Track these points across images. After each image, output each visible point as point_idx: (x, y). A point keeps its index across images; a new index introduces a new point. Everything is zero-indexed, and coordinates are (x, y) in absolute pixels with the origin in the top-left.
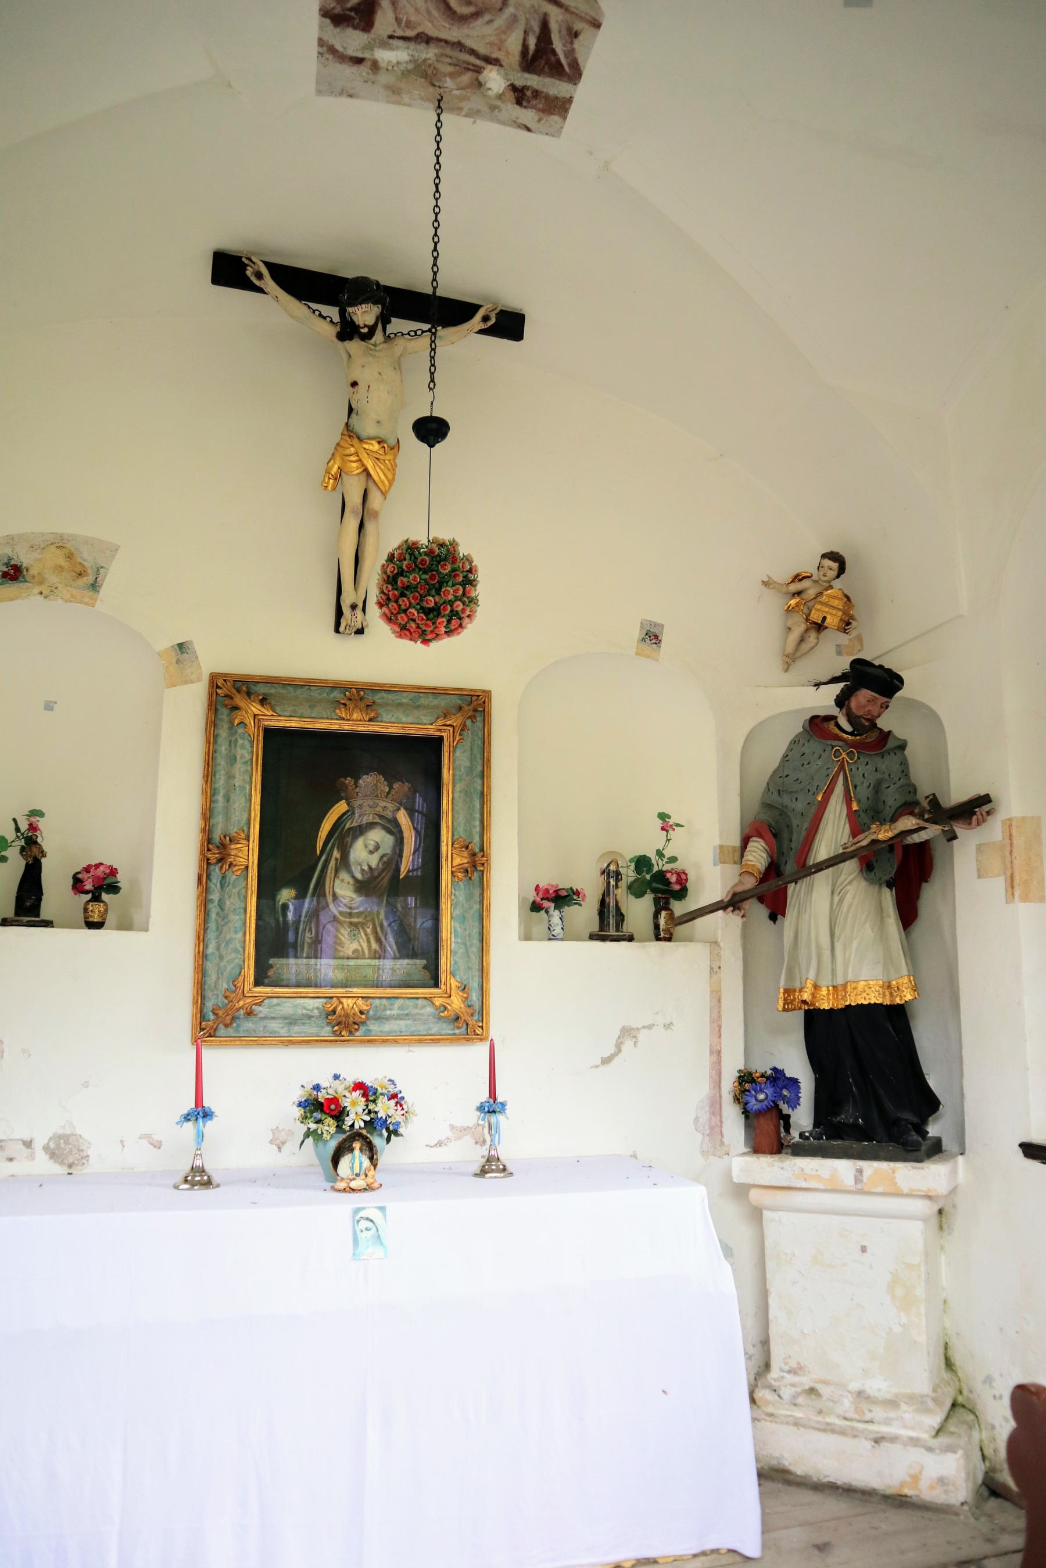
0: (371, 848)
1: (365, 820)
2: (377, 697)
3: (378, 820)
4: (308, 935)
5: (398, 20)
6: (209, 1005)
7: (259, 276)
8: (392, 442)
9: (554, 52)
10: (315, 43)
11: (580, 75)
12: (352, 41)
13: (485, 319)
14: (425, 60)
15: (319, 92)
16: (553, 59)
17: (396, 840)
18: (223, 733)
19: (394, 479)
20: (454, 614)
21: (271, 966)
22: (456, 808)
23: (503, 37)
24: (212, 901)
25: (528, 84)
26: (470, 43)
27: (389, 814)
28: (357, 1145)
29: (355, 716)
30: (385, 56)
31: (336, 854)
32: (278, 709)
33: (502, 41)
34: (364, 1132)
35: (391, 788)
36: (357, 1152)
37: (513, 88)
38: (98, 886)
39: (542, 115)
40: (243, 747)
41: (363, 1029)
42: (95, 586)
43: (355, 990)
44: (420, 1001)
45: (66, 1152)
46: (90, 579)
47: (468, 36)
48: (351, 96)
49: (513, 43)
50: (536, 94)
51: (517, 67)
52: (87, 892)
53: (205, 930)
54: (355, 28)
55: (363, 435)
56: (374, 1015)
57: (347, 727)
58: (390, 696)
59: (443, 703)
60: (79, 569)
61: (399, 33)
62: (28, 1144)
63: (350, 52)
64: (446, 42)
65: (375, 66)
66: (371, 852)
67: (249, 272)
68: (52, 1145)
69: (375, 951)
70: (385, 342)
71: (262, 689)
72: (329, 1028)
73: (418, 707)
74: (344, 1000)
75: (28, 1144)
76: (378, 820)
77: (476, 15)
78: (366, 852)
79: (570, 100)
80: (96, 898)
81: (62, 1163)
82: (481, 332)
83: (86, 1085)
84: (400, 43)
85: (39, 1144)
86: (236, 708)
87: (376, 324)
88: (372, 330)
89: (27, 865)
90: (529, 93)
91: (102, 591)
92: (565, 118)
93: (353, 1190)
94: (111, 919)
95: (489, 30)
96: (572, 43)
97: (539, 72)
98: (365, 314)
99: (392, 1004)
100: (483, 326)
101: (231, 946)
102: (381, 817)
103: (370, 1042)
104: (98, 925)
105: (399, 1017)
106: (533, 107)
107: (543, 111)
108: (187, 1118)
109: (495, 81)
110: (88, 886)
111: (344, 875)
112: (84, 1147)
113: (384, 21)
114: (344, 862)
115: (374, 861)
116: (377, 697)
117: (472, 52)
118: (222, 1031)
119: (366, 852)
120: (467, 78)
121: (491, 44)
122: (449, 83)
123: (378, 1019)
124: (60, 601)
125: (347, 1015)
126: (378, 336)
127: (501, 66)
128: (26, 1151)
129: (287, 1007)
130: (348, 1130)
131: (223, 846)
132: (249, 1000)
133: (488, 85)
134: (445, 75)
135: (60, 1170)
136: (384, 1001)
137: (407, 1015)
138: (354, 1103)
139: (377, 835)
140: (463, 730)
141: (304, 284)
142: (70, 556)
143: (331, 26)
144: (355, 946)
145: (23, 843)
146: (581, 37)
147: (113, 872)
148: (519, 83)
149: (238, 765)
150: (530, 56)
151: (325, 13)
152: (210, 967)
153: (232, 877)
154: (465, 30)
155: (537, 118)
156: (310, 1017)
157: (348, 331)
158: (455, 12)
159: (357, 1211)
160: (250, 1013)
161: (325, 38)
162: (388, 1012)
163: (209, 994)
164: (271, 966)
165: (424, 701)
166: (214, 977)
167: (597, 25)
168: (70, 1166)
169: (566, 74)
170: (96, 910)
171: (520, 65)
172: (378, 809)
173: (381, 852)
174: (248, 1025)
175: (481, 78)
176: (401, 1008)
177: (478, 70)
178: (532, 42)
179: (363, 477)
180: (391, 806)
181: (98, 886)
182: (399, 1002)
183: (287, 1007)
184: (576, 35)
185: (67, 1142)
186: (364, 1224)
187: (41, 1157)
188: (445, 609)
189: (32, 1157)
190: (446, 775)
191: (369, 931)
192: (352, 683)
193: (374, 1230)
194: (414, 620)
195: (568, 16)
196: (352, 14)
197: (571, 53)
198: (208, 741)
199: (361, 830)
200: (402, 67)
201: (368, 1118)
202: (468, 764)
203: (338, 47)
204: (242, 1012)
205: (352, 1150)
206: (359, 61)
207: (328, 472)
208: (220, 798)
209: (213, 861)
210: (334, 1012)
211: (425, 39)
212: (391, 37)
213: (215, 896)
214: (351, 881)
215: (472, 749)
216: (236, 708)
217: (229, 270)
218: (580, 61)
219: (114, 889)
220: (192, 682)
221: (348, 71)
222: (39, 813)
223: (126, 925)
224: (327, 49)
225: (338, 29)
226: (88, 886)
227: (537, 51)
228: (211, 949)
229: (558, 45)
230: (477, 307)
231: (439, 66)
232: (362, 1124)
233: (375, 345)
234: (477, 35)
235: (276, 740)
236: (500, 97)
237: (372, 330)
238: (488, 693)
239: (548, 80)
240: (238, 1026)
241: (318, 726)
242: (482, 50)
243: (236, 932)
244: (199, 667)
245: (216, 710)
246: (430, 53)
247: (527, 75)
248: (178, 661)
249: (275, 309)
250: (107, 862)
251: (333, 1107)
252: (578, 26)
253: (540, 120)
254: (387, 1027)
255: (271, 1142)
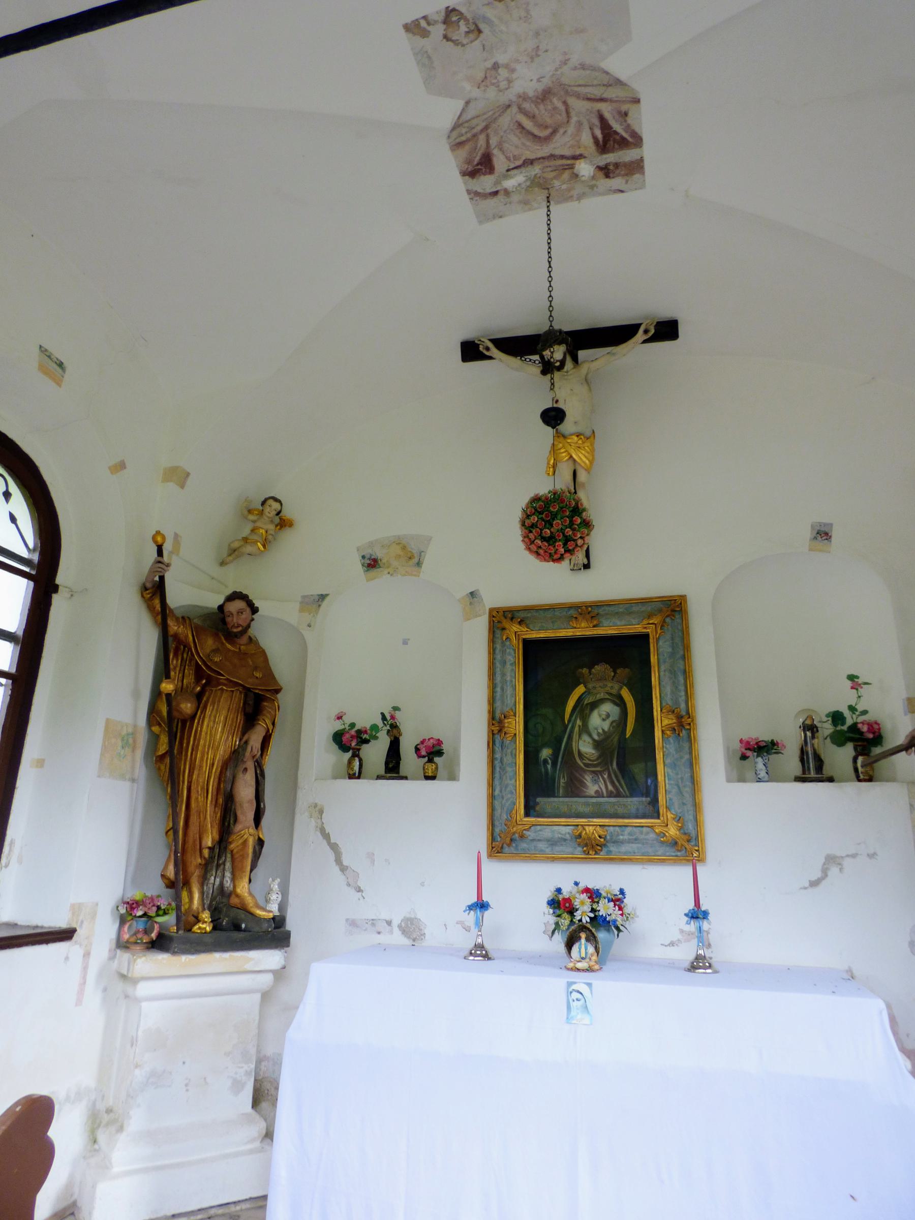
0: (604, 717)
1: (598, 697)
2: (601, 611)
3: (608, 697)
4: (562, 781)
5: (508, 158)
6: (497, 830)
7: (488, 349)
8: (588, 433)
9: (616, 133)
10: (465, 193)
11: (641, 139)
12: (486, 183)
13: (646, 332)
14: (536, 175)
15: (480, 222)
16: (618, 137)
17: (621, 709)
18: (498, 646)
19: (593, 458)
20: (567, 540)
21: (538, 804)
22: (662, 683)
23: (577, 138)
24: (496, 759)
25: (608, 161)
26: (558, 152)
27: (614, 691)
28: (583, 935)
29: (583, 625)
30: (509, 184)
31: (579, 722)
32: (531, 626)
33: (578, 141)
34: (588, 926)
35: (615, 673)
36: (583, 941)
37: (600, 168)
38: (432, 752)
39: (626, 178)
40: (510, 654)
41: (605, 850)
42: (419, 564)
43: (595, 820)
44: (644, 829)
45: (411, 929)
46: (416, 560)
47: (517, 147)
48: (501, 217)
49: (586, 139)
50: (617, 165)
51: (596, 154)
52: (424, 757)
53: (493, 779)
54: (484, 174)
55: (566, 433)
56: (611, 839)
57: (579, 633)
58: (612, 609)
59: (649, 609)
60: (409, 555)
61: (512, 166)
62: (389, 923)
63: (488, 190)
64: (543, 158)
65: (507, 192)
66: (604, 720)
67: (481, 348)
68: (403, 925)
69: (611, 792)
70: (574, 368)
71: (522, 615)
72: (580, 849)
73: (630, 613)
74: (587, 828)
75: (389, 923)
76: (608, 697)
77: (555, 132)
78: (601, 720)
79: (642, 160)
80: (430, 761)
81: (409, 938)
82: (645, 342)
83: (422, 884)
84: (515, 171)
85: (396, 923)
86: (504, 629)
87: (565, 357)
88: (563, 362)
89: (391, 742)
90: (611, 167)
91: (423, 566)
92: (643, 173)
93: (578, 970)
94: (441, 772)
95: (566, 138)
96: (626, 121)
97: (612, 150)
98: (558, 353)
99: (623, 831)
100: (646, 337)
101: (508, 789)
102: (610, 694)
103: (611, 860)
104: (433, 778)
105: (629, 842)
106: (618, 175)
107: (627, 175)
108: (471, 908)
109: (585, 169)
110: (423, 753)
111: (585, 737)
112: (422, 927)
113: (500, 162)
114: (585, 729)
115: (606, 726)
116: (601, 611)
117: (563, 157)
118: (506, 849)
119: (601, 720)
120: (566, 175)
121: (572, 146)
122: (556, 183)
123: (616, 842)
124: (399, 576)
125: (589, 839)
126: (569, 364)
127: (585, 157)
128: (388, 928)
129: (547, 833)
130: (585, 926)
131: (501, 722)
132: (520, 827)
133: (581, 174)
134: (552, 179)
135: (406, 941)
136: (617, 828)
137: (636, 839)
138: (582, 903)
139: (607, 708)
140: (662, 626)
141: (517, 346)
142: (404, 548)
143: (471, 180)
144: (596, 788)
145: (388, 727)
146: (630, 114)
147: (439, 742)
148: (602, 164)
149: (508, 666)
150: (601, 142)
151: (464, 174)
152: (496, 803)
153: (507, 742)
154: (552, 146)
155: (624, 181)
156: (565, 840)
157: (548, 368)
158: (540, 137)
159: (570, 984)
160: (522, 836)
161: (470, 188)
162: (621, 837)
163: (497, 823)
164: (538, 804)
165: (635, 609)
166: (499, 811)
167: (637, 101)
168: (414, 940)
169: (631, 143)
170: (430, 768)
171: (598, 151)
172: (608, 689)
173: (611, 719)
174: (524, 845)
175: (575, 171)
176: (630, 834)
177: (571, 167)
178: (598, 133)
179: (571, 462)
180: (616, 686)
181: (432, 752)
182: (629, 829)
183: (547, 833)
184: (626, 114)
185: (412, 924)
186: (575, 995)
187: (397, 931)
188: (559, 536)
189: (391, 932)
190: (653, 659)
191: (606, 776)
192: (583, 603)
193: (583, 1001)
194: (540, 547)
195: (614, 105)
196: (479, 167)
197: (628, 128)
198: (489, 653)
199: (594, 705)
200: (523, 186)
201: (592, 915)
202: (670, 650)
203: (480, 190)
204: (517, 835)
205: (580, 938)
206: (496, 193)
207: (548, 464)
208: (498, 689)
209: (496, 732)
210: (580, 836)
211: (529, 162)
212: (508, 170)
213: (498, 756)
214: (591, 741)
215: (672, 639)
216: (504, 629)
217: (471, 351)
218: (637, 130)
219: (440, 753)
220: (480, 616)
221: (492, 202)
222: (396, 709)
223: (453, 777)
224: (475, 195)
225: (475, 180)
226: (423, 753)
227: (604, 137)
228: (497, 792)
229: (617, 127)
230: (638, 326)
231: (545, 175)
232: (588, 920)
233: (567, 372)
234: (561, 145)
235: (529, 646)
236: (593, 178)
237: (563, 362)
238: (683, 598)
239: (621, 153)
240: (517, 846)
241: (558, 635)
242: (567, 152)
243: (511, 779)
244: (484, 605)
245: (494, 632)
246: (536, 170)
247: (605, 156)
248: (471, 603)
249: (502, 369)
250: (436, 737)
251: (567, 905)
252: (624, 108)
253: (627, 182)
254: (624, 848)
255: (544, 932)
